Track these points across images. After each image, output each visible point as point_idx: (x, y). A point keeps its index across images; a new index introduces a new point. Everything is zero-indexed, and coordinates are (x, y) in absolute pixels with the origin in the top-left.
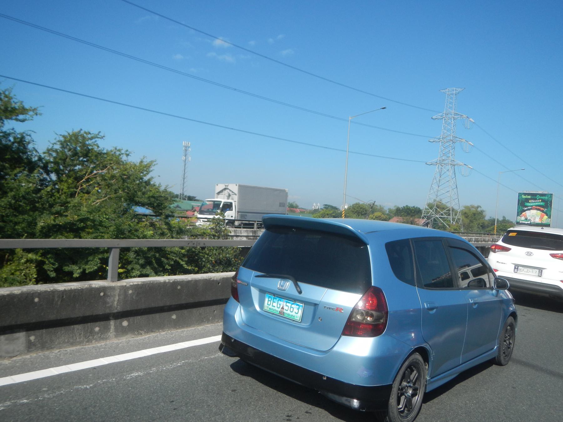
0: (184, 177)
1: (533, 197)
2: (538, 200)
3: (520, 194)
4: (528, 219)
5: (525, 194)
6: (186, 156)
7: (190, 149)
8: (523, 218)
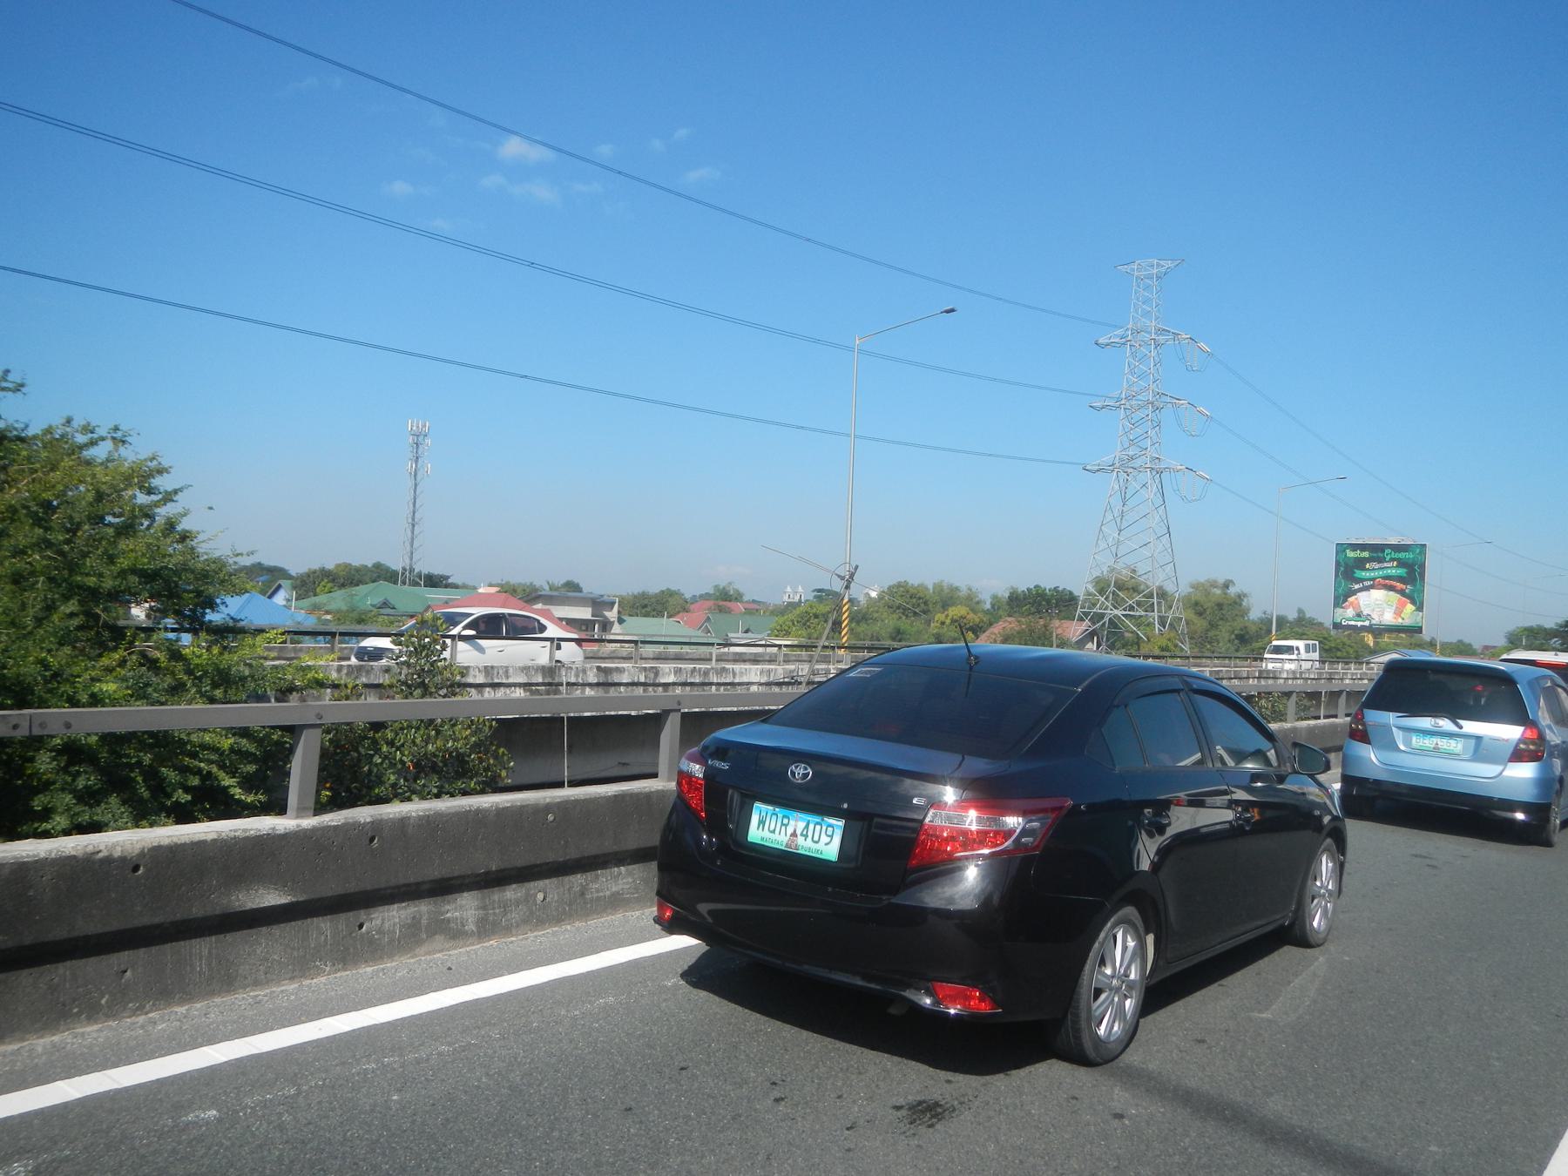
0: (413, 520)
1: (1375, 555)
3: (1341, 548)
4: (1365, 613)
5: (1354, 547)
6: (416, 462)
7: (429, 441)
8: (1350, 612)
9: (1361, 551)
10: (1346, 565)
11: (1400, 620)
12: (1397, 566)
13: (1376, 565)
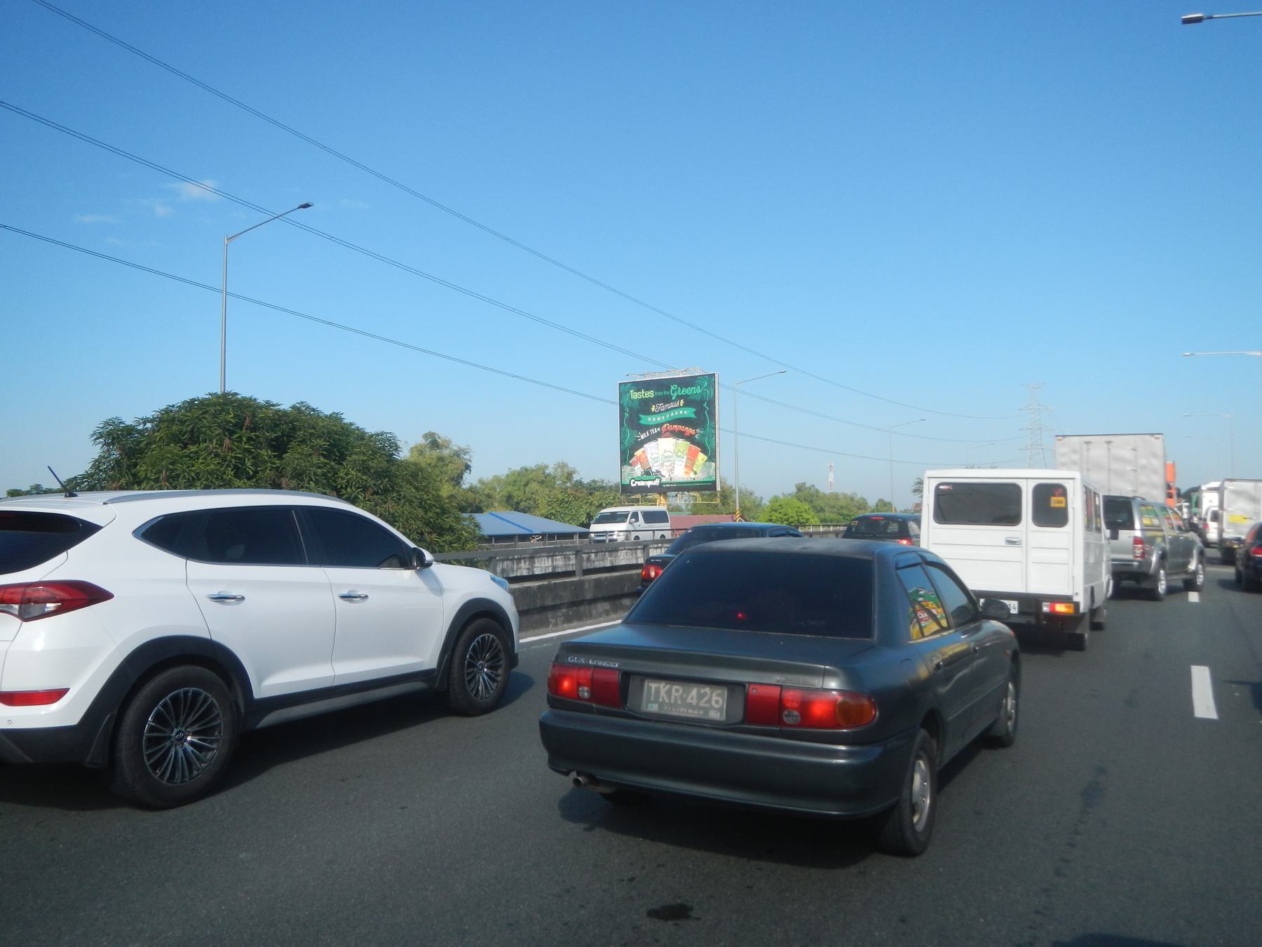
1: (660, 393)
2: (676, 401)
3: (624, 388)
5: (639, 386)
9: (646, 390)
10: (631, 409)
11: (692, 475)
12: (685, 405)
13: (662, 407)
